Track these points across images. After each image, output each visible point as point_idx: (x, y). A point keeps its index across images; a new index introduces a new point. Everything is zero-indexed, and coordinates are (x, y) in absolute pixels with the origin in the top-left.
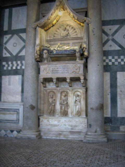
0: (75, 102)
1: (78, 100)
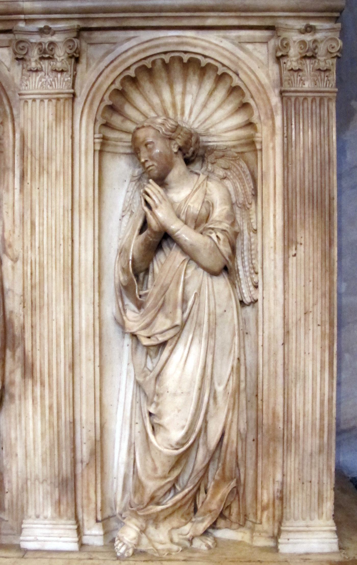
0: (139, 271)
1: (200, 222)
